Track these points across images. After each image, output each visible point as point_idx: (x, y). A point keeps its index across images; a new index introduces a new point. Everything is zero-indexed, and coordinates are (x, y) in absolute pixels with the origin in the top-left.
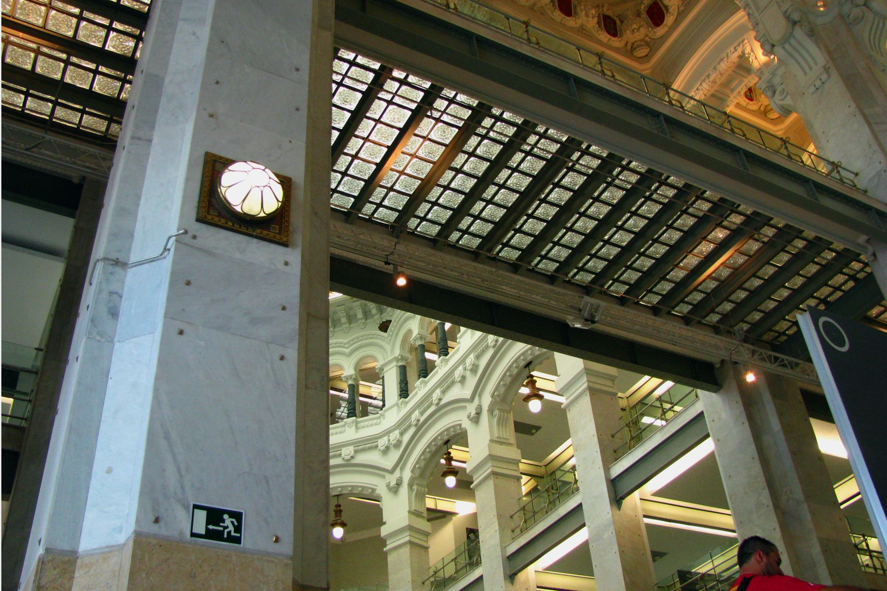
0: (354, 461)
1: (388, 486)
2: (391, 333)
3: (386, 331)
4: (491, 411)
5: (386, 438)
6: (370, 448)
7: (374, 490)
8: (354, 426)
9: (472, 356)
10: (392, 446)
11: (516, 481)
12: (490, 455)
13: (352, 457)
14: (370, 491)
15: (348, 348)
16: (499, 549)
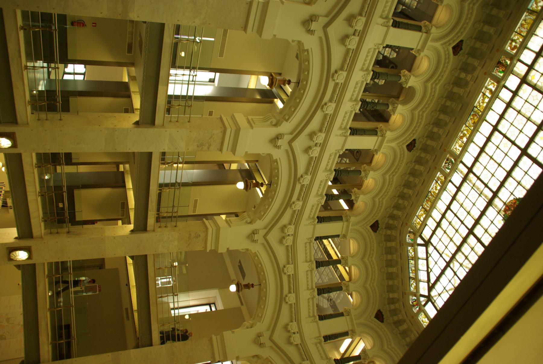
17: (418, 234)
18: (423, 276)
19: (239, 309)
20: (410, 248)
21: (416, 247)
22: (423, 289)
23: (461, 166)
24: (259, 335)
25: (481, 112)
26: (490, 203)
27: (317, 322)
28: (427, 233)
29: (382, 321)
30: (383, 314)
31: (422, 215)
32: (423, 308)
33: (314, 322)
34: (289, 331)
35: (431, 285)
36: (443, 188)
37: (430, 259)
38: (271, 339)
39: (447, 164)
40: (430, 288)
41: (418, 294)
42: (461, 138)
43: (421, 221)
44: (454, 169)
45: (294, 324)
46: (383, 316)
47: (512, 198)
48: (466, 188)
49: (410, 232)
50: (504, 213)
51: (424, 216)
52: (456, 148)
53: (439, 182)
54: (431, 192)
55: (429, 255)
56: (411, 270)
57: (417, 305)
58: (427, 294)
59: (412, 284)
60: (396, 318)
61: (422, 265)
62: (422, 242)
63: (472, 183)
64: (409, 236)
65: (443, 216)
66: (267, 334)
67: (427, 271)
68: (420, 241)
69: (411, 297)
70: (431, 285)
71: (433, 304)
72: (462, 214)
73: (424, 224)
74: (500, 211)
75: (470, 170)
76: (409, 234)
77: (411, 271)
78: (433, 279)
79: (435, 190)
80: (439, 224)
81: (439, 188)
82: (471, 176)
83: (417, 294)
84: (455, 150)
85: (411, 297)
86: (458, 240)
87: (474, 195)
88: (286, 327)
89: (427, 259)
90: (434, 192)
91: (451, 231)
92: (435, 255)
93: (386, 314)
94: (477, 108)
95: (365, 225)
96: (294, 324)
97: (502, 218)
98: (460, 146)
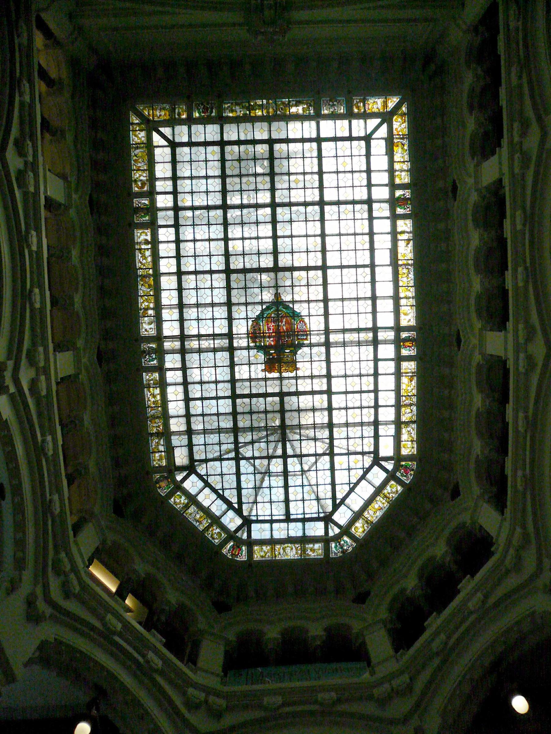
18: (217, 508)
25: (150, 269)
31: (158, 444)
35: (236, 506)
37: (211, 480)
40: (239, 512)
43: (161, 452)
44: (161, 353)
49: (157, 482)
54: (149, 407)
55: (205, 477)
56: (197, 521)
59: (211, 537)
64: (160, 487)
70: (236, 506)
73: (170, 450)
76: (158, 485)
79: (153, 400)
80: (190, 432)
89: (207, 484)
94: (142, 269)
98: (150, 323)
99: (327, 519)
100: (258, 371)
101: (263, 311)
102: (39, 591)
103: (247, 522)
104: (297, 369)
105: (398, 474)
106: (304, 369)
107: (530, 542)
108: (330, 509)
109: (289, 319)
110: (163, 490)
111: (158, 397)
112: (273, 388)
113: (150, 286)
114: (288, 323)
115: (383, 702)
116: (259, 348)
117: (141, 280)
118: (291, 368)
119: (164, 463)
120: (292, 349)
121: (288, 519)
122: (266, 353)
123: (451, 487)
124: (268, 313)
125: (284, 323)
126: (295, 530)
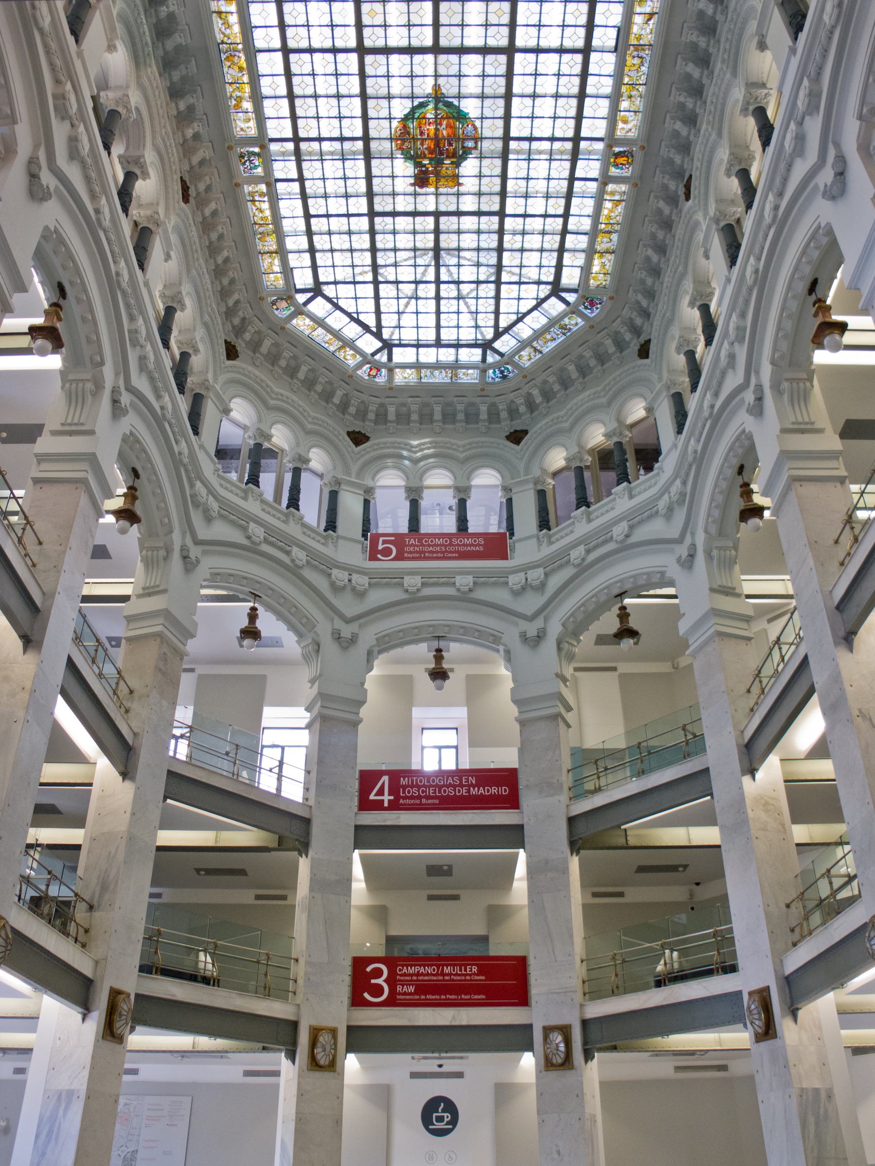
0: (633, 539)
1: (679, 560)
2: (654, 356)
3: (647, 357)
4: (776, 387)
5: (666, 496)
6: (650, 517)
7: (663, 573)
8: (626, 495)
9: (734, 318)
10: (675, 505)
11: (838, 485)
12: (782, 452)
13: (627, 536)
14: (658, 576)
15: (605, 396)
16: (819, 597)
17: (293, 291)
18: (352, 330)
19: (201, 678)
20: (294, 322)
21: (305, 309)
22: (369, 344)
23: (274, 147)
24: (337, 636)
26: (368, 156)
27: (338, 537)
28: (303, 278)
29: (367, 439)
30: (357, 430)
31: (271, 264)
32: (392, 364)
33: (337, 541)
34: (344, 587)
35: (374, 330)
36: (274, 199)
37: (342, 303)
38: (348, 621)
39: (247, 163)
40: (378, 335)
41: (370, 357)
42: (238, 106)
45: (335, 572)
46: (359, 433)
47: (395, 124)
48: (311, 169)
49: (274, 303)
50: (400, 152)
51: (277, 262)
52: (242, 129)
53: (257, 198)
54: (255, 224)
55: (335, 300)
57: (378, 370)
58: (379, 344)
59: (344, 358)
60: (371, 416)
61: (337, 321)
62: (309, 295)
63: (316, 155)
64: (277, 309)
65: (309, 233)
66: (339, 624)
67: (352, 319)
68: (301, 298)
69: (359, 372)
70: (374, 330)
71: (400, 345)
72: (336, 206)
73: (287, 272)
74: (392, 154)
75: (296, 139)
76: (275, 307)
77: (326, 346)
78: (371, 321)
79: (261, 215)
81: (265, 206)
82: (303, 146)
83: (367, 359)
84: (242, 133)
85: (359, 372)
86: (364, 241)
87: (332, 168)
88: (336, 589)
89: (337, 307)
90: (262, 219)
91: (340, 242)
92: (345, 291)
93: (357, 426)
95: (223, 366)
96: (335, 572)
97: (402, 160)
99: (486, 346)
100: (403, 185)
101: (413, 109)
102: (189, 542)
103: (388, 346)
104: (459, 184)
105: (581, 308)
106: (469, 184)
107: (684, 501)
108: (489, 334)
109: (451, 121)
110: (283, 311)
111: (268, 213)
112: (428, 203)
113: (241, 69)
114: (451, 127)
115: (517, 593)
116: (408, 157)
117: (227, 59)
118: (451, 184)
119: (281, 283)
120: (454, 160)
121: (438, 343)
122: (418, 165)
123: (642, 339)
124: (420, 111)
125: (444, 126)
126: (447, 355)
